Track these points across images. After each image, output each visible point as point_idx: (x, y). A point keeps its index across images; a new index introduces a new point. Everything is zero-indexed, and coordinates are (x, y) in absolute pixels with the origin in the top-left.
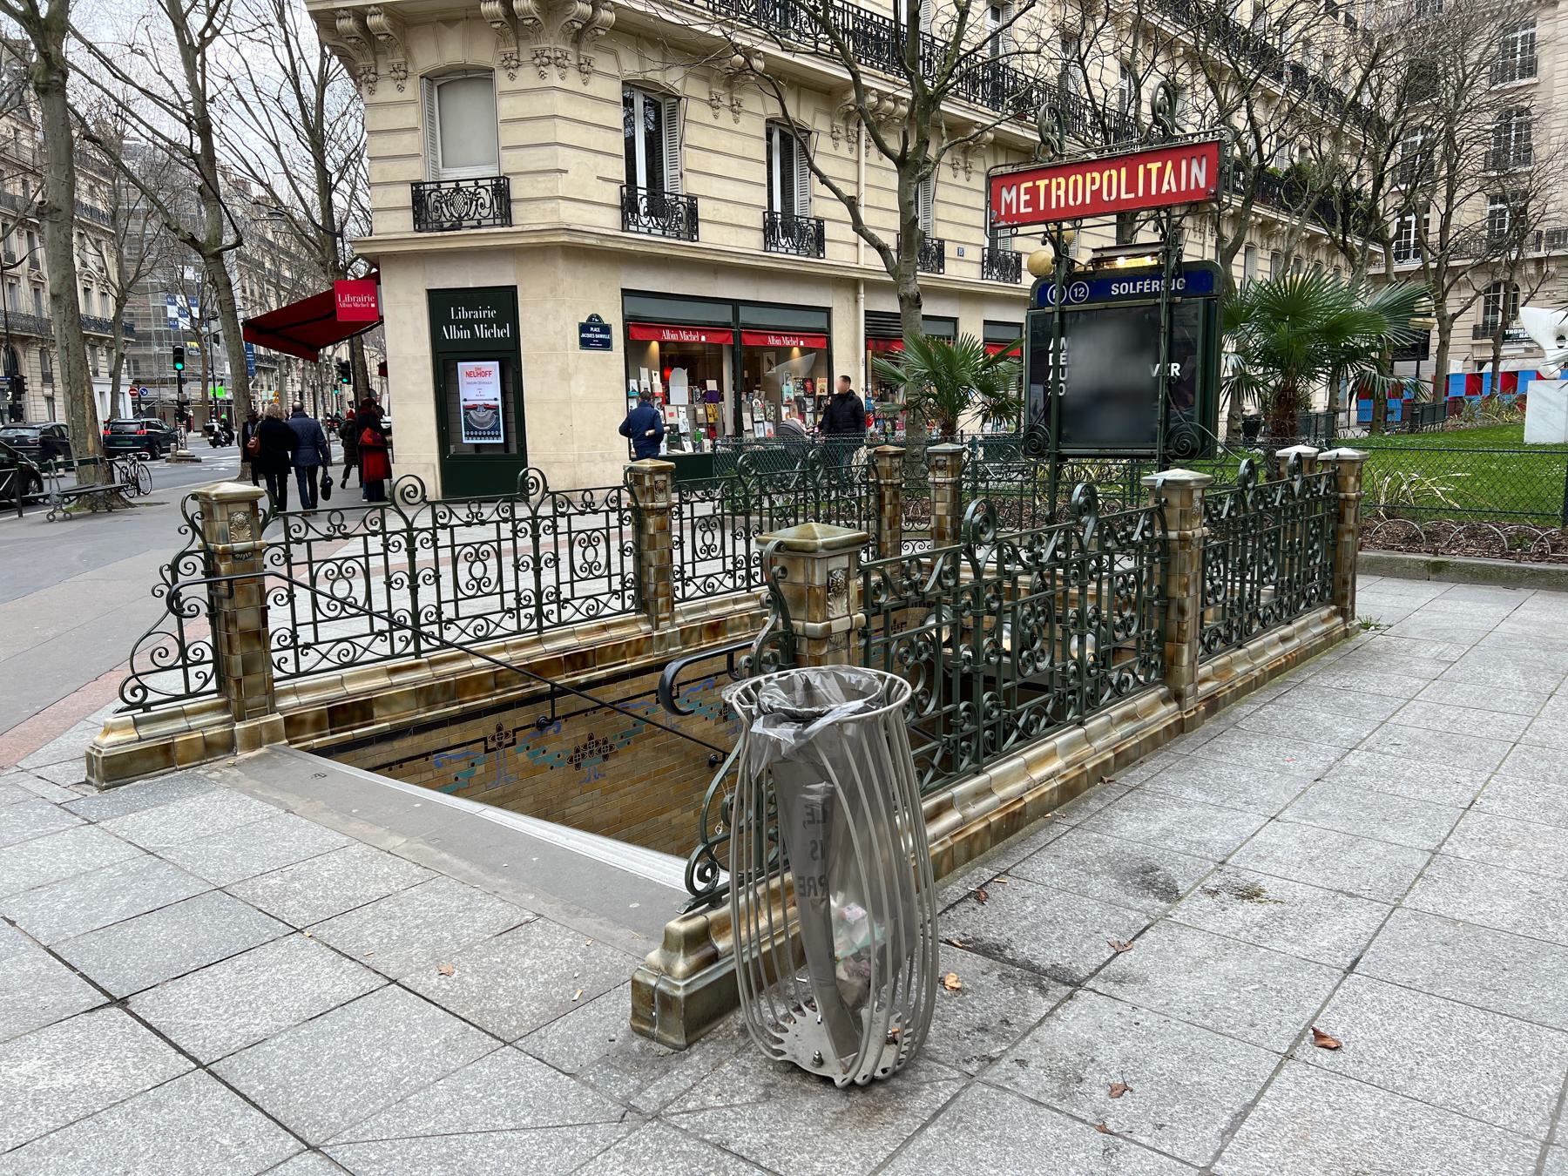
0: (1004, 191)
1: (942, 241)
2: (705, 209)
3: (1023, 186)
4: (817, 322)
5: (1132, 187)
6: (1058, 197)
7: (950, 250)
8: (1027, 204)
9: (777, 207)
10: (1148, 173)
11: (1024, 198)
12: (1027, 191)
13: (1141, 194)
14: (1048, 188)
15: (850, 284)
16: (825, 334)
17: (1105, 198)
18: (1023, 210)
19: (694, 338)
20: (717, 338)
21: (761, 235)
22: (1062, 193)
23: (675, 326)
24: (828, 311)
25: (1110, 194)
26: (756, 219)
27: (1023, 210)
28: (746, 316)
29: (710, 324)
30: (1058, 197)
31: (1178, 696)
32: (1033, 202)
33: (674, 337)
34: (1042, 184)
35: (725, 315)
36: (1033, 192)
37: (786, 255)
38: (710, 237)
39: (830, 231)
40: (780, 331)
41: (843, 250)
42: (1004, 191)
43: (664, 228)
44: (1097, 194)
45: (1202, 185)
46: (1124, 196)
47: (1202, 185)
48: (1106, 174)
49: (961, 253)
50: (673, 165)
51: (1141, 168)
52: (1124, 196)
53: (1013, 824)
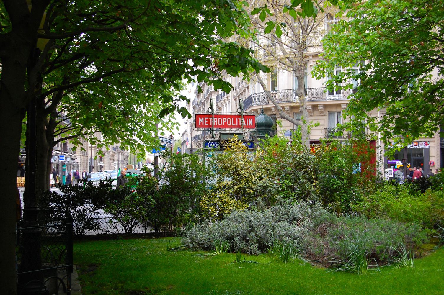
0: (200, 118)
3: (205, 118)
5: (235, 123)
6: (215, 123)
8: (207, 123)
10: (239, 120)
11: (206, 121)
12: (207, 120)
13: (237, 125)
14: (212, 120)
17: (228, 124)
18: (205, 124)
22: (216, 121)
25: (229, 123)
27: (205, 124)
30: (215, 123)
34: (211, 119)
36: (209, 120)
42: (200, 118)
44: (226, 123)
45: (252, 125)
46: (233, 125)
47: (252, 125)
48: (228, 119)
51: (237, 119)
52: (233, 125)
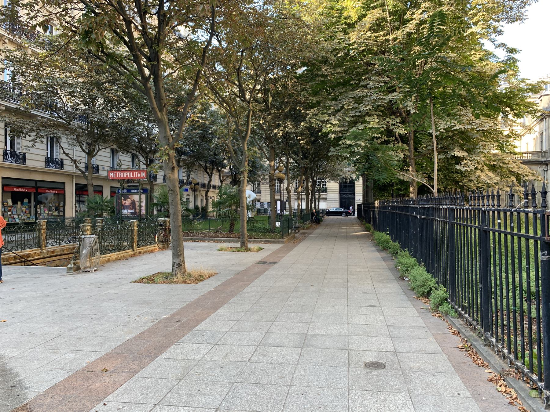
1: (98, 165)
2: (28, 156)
4: (61, 186)
5: (133, 175)
7: (100, 168)
9: (49, 156)
15: (71, 176)
16: (64, 189)
19: (23, 190)
20: (30, 191)
21: (44, 163)
23: (18, 187)
24: (64, 183)
26: (44, 159)
28: (39, 184)
29: (28, 186)
31: (134, 251)
32: (116, 176)
33: (17, 190)
35: (33, 184)
37: (52, 168)
38: (29, 163)
39: (65, 162)
40: (50, 189)
41: (69, 167)
43: (16, 161)
44: (127, 176)
49: (103, 168)
50: (19, 144)
53: (108, 261)
